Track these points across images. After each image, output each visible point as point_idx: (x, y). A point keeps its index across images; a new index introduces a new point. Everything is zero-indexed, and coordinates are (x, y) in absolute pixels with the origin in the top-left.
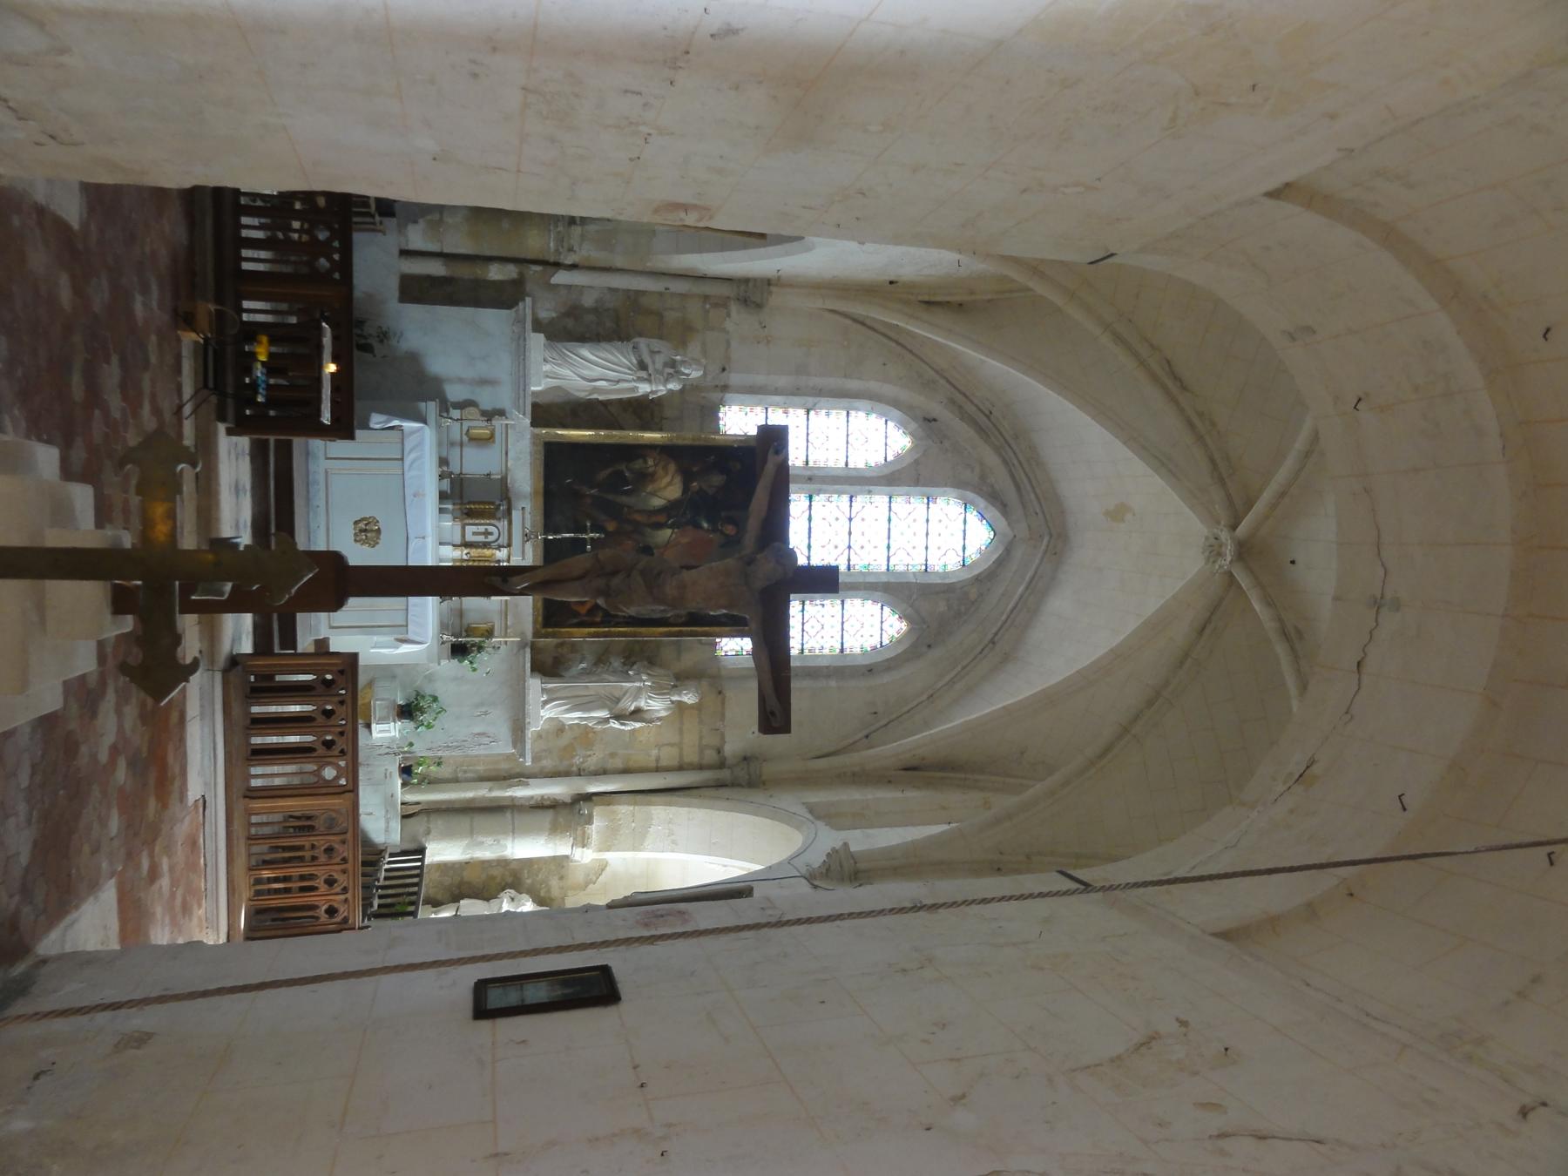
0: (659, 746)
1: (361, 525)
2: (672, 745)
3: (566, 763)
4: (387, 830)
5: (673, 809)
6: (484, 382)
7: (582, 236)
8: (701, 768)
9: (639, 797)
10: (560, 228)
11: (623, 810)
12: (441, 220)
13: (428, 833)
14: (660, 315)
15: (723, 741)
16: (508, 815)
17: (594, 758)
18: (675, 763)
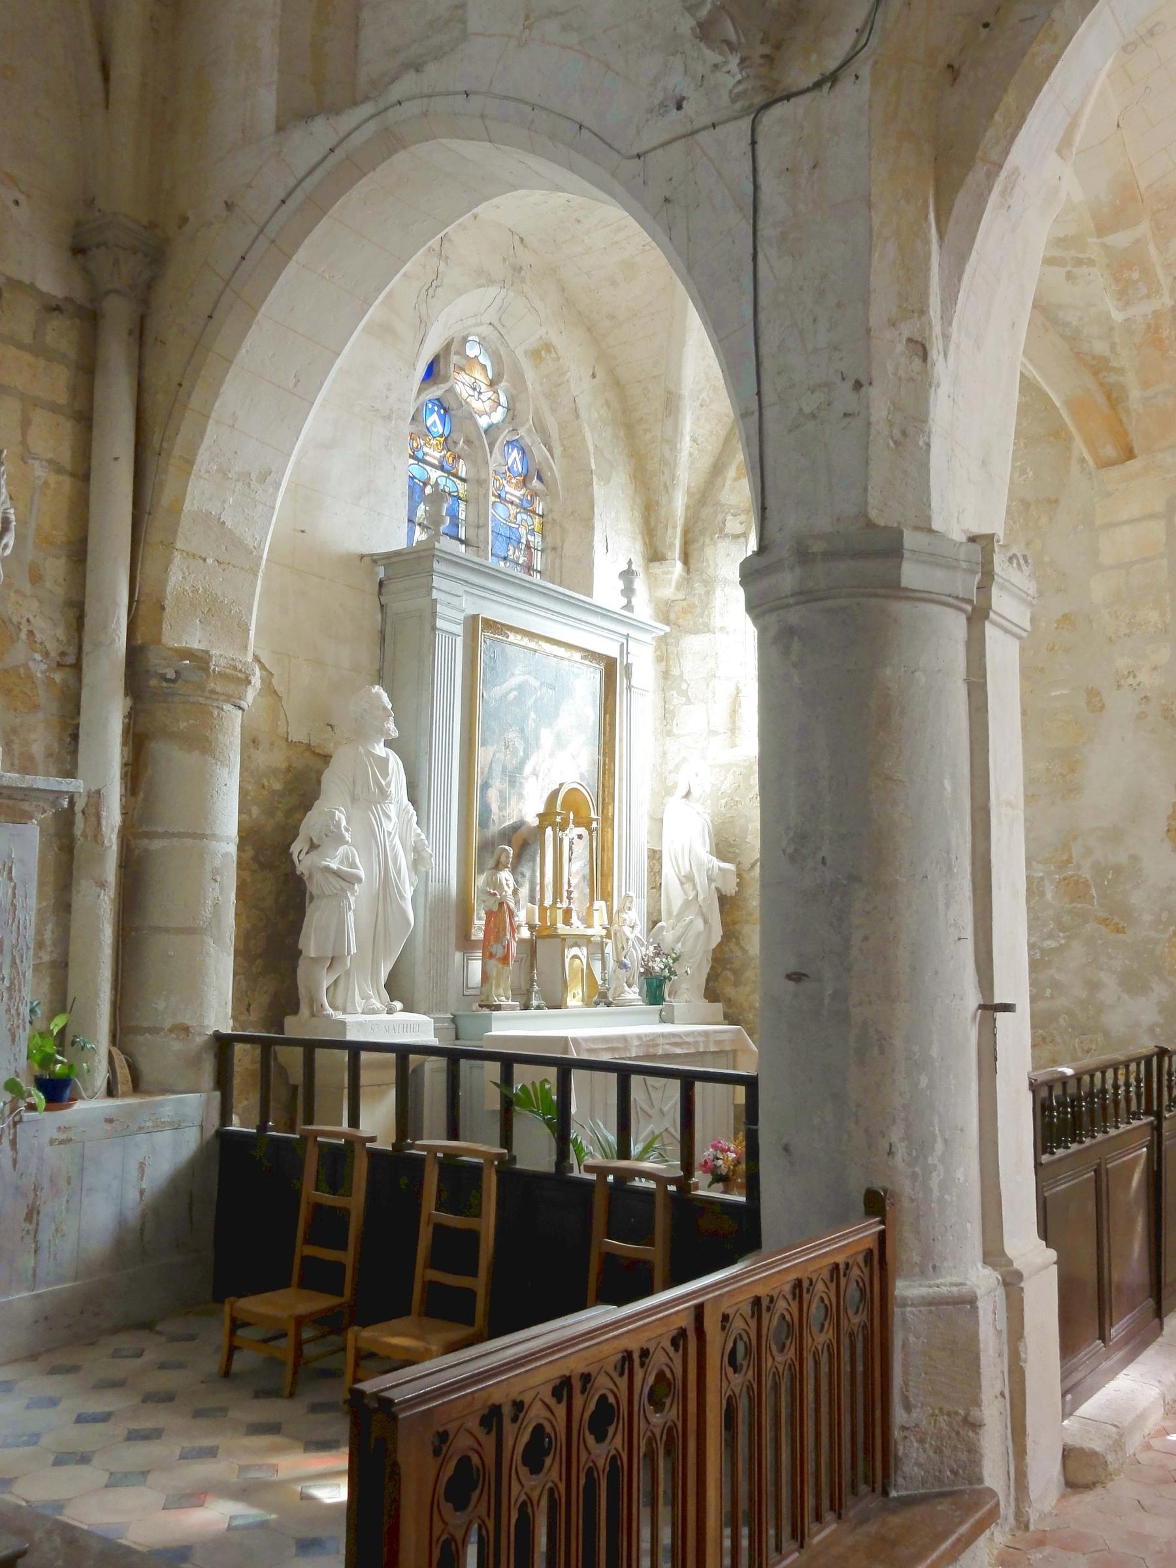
0: (26, 455)
2: (26, 423)
3: (43, 696)
4: (177, 1126)
5: (203, 456)
8: (88, 369)
9: (154, 534)
11: (178, 579)
16: (156, 845)
17: (39, 623)
18: (67, 427)
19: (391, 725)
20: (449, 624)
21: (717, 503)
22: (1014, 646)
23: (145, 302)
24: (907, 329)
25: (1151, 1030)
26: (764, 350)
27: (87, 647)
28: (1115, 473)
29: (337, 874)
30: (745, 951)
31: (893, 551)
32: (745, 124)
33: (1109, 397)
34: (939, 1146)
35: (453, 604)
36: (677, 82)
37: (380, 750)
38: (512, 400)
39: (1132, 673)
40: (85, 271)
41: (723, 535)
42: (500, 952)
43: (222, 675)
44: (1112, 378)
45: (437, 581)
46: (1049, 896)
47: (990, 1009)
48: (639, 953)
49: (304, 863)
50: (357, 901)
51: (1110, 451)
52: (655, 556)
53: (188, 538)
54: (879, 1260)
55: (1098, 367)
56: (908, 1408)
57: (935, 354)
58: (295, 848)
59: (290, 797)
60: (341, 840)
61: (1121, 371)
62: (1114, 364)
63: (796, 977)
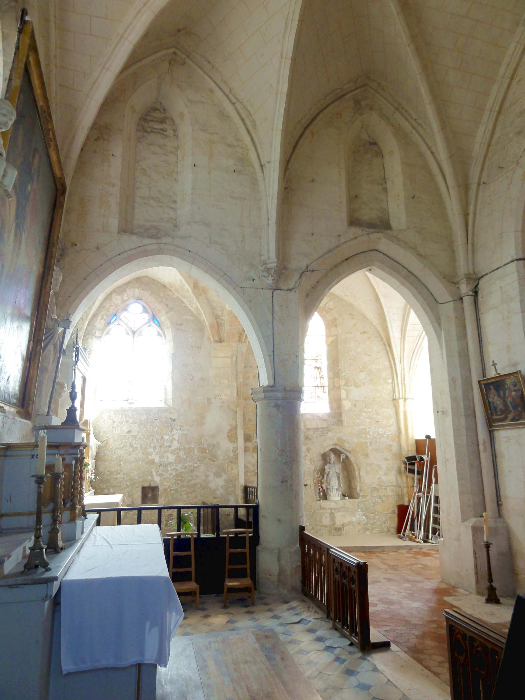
21: (94, 326)
25: (222, 487)
26: (275, 343)
28: (219, 344)
33: (218, 325)
36: (252, 274)
39: (220, 395)
41: (95, 337)
44: (220, 321)
46: (196, 452)
51: (217, 338)
55: (217, 317)
61: (223, 320)
62: (221, 318)
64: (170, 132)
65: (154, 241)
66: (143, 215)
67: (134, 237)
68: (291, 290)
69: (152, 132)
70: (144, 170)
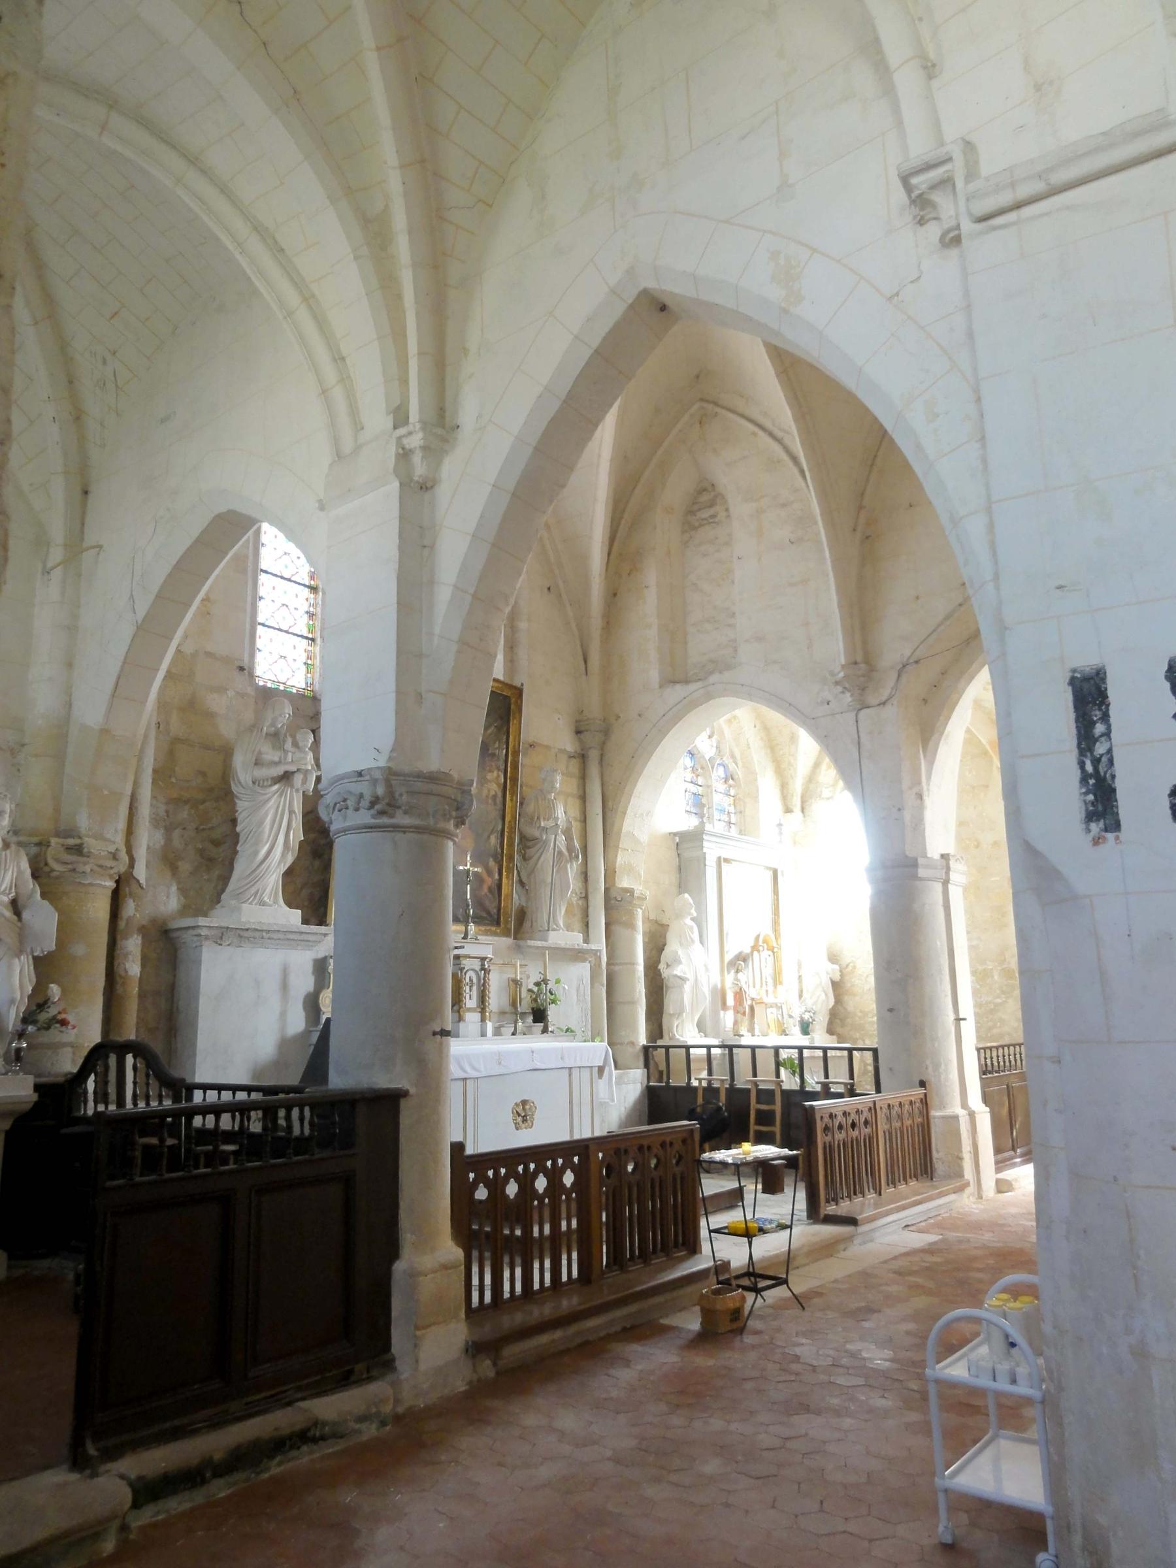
1: (519, 1119)
6: (285, 986)
7: (99, 837)
8: (583, 777)
10: (88, 869)
11: (621, 859)
12: (72, 1045)
13: (633, 1043)
14: (176, 740)
15: (562, 751)
16: (617, 968)
18: (578, 802)
19: (693, 911)
20: (711, 862)
22: (960, 890)
23: (602, 749)
24: (915, 790)
27: (590, 890)
29: (680, 978)
30: (845, 1009)
31: (913, 864)
32: (854, 714)
34: (943, 1067)
35: (712, 850)
37: (688, 921)
38: (719, 742)
40: (580, 741)
42: (742, 1010)
43: (639, 898)
45: (705, 844)
46: (996, 977)
47: (958, 1020)
48: (797, 1011)
49: (665, 973)
50: (687, 987)
52: (788, 810)
53: (624, 843)
54: (925, 1101)
56: (938, 1152)
57: (925, 798)
58: (661, 966)
59: (656, 946)
60: (680, 962)
63: (891, 1010)
64: (722, 515)
65: (699, 684)
66: (702, 645)
67: (678, 687)
68: (884, 703)
69: (701, 525)
70: (694, 584)
